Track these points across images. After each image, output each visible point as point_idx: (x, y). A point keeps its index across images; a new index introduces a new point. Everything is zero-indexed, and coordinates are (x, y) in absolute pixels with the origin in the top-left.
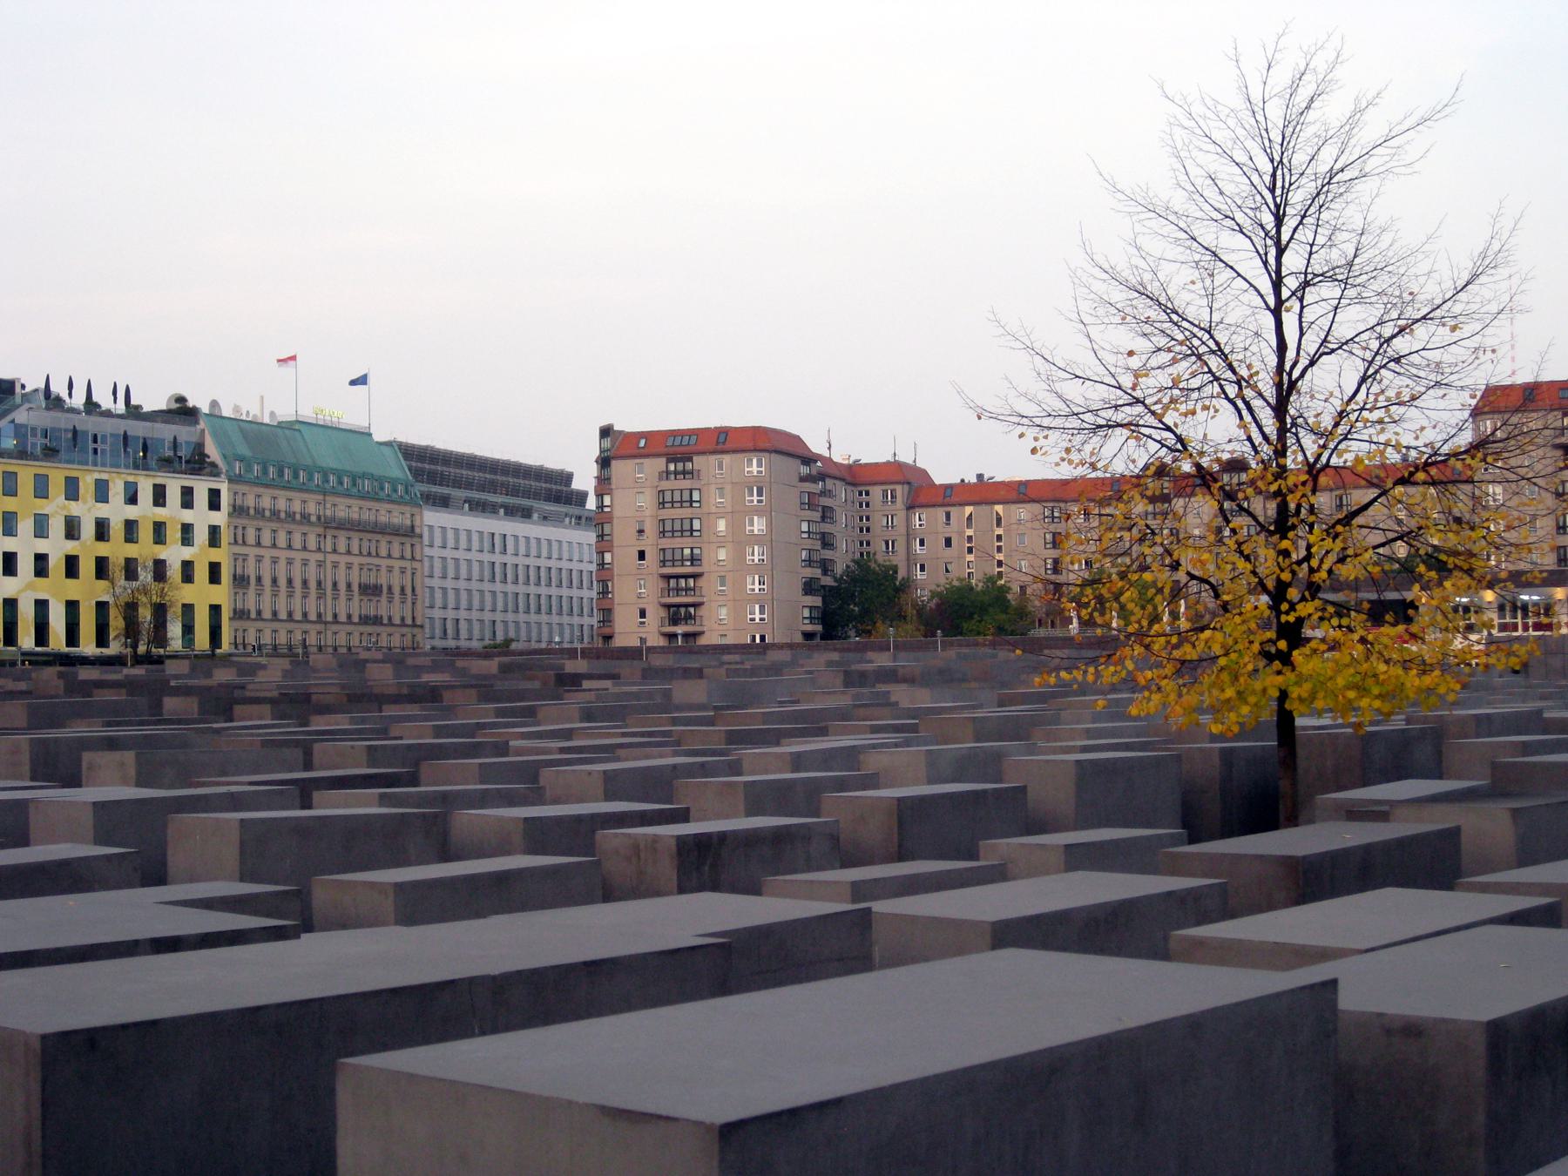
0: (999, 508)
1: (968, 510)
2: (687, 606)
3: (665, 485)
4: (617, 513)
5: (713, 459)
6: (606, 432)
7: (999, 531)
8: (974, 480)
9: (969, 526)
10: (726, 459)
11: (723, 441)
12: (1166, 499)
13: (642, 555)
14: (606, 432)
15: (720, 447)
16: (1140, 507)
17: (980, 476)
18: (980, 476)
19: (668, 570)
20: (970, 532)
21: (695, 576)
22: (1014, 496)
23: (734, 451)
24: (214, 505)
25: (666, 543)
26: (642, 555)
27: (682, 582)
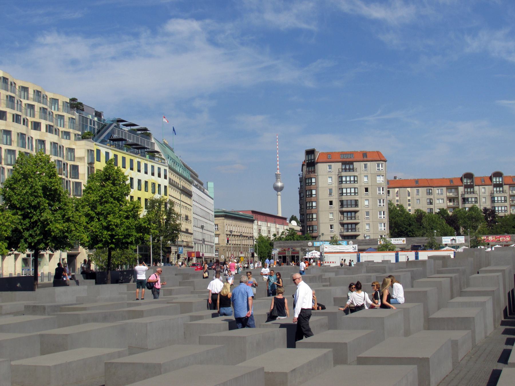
0: (409, 189)
1: (397, 190)
2: (351, 224)
3: (344, 174)
4: (320, 184)
5: (362, 164)
6: (310, 152)
7: (409, 198)
8: (393, 179)
9: (397, 196)
10: (369, 164)
11: (365, 157)
12: (471, 186)
13: (331, 203)
14: (310, 152)
15: (365, 159)
16: (461, 189)
17: (395, 178)
18: (395, 178)
19: (344, 209)
20: (397, 198)
21: (356, 212)
22: (415, 185)
23: (372, 161)
24: (165, 177)
25: (344, 198)
26: (331, 203)
27: (349, 214)
